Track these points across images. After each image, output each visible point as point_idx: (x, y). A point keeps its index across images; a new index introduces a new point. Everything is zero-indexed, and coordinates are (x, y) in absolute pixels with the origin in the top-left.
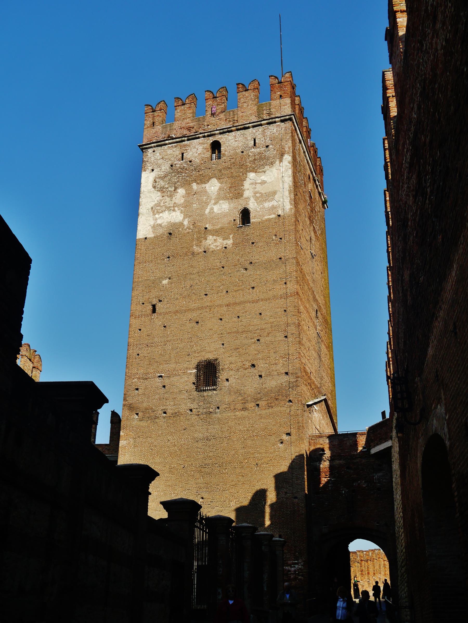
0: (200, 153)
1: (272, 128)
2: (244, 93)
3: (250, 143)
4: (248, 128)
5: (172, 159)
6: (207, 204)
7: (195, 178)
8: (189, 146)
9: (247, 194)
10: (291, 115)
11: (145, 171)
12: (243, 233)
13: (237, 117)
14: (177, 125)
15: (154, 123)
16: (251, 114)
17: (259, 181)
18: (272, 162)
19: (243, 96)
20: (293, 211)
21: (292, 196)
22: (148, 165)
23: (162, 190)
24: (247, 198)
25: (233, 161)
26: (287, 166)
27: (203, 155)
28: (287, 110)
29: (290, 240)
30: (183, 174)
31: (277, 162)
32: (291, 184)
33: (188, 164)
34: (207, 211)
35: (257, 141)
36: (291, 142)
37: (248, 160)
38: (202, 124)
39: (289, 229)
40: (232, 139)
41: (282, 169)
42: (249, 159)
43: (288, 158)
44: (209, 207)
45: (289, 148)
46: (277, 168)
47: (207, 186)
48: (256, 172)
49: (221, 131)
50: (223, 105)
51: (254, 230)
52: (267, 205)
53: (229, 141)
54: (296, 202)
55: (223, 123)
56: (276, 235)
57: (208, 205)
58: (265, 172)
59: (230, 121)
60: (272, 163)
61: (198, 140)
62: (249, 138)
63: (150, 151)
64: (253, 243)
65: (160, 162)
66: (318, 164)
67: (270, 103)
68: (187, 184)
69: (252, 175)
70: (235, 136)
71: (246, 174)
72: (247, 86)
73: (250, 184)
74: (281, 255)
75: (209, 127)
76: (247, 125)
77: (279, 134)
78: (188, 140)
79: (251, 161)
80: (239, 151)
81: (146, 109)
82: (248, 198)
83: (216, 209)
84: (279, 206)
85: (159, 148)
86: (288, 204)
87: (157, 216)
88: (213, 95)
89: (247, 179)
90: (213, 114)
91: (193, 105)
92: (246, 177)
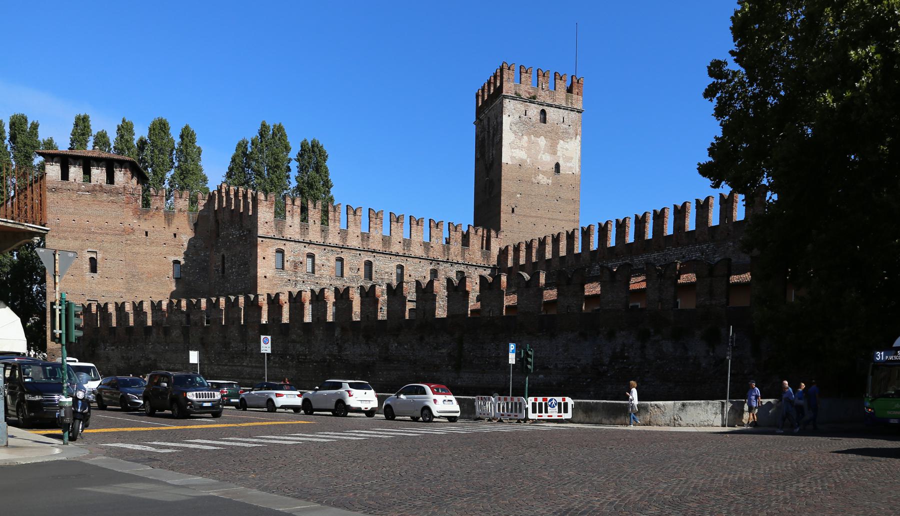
9: (559, 153)
23: (515, 132)
31: (574, 139)
34: (539, 157)
43: (579, 137)
44: (540, 155)
47: (539, 140)
60: (571, 138)
68: (529, 134)
69: (561, 142)
80: (556, 122)
87: (512, 150)
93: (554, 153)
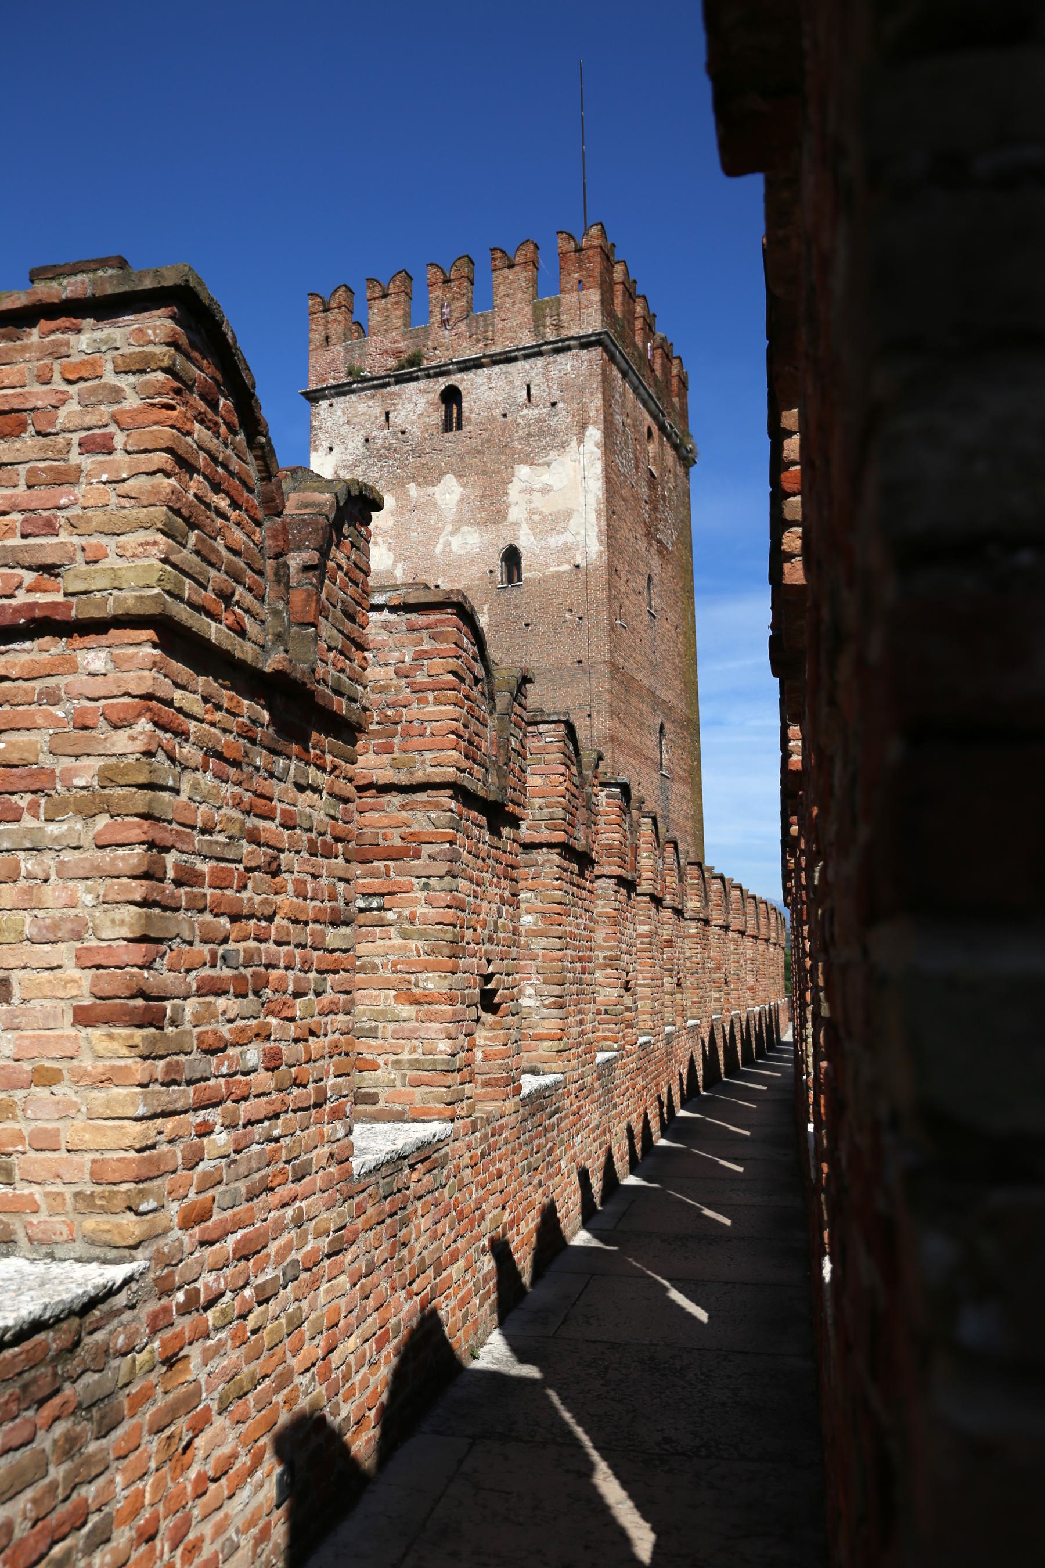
0: (422, 414)
1: (563, 361)
2: (505, 271)
3: (519, 395)
4: (515, 359)
5: (368, 425)
6: (438, 532)
7: (413, 471)
8: (399, 395)
9: (514, 514)
10: (600, 334)
11: (316, 450)
12: (508, 600)
13: (493, 332)
14: (375, 343)
15: (327, 338)
16: (521, 326)
17: (538, 486)
18: (563, 443)
19: (505, 278)
20: (605, 558)
21: (604, 523)
22: (322, 436)
24: (515, 524)
25: (486, 435)
26: (592, 453)
27: (427, 420)
28: (592, 322)
29: (598, 623)
30: (391, 462)
31: (574, 443)
32: (600, 494)
33: (398, 439)
34: (439, 548)
35: (533, 392)
36: (600, 396)
37: (516, 436)
38: (424, 346)
39: (596, 598)
40: (483, 384)
41: (584, 461)
42: (517, 432)
43: (594, 434)
44: (442, 540)
45: (597, 411)
46: (574, 458)
47: (437, 490)
48: (532, 464)
49: (461, 366)
50: (465, 299)
51: (529, 597)
52: (555, 541)
53: (478, 388)
54: (611, 537)
55: (464, 345)
56: (571, 611)
57: (439, 534)
58: (549, 464)
59: (478, 341)
60: (563, 445)
61: (416, 383)
62: (517, 383)
63: (324, 404)
64: (527, 625)
65: (345, 430)
66: (675, 372)
67: (559, 300)
69: (523, 471)
70: (489, 378)
71: (512, 468)
72: (510, 254)
73: (520, 492)
74: (582, 654)
75: (437, 352)
76: (513, 354)
77: (577, 376)
78: (397, 383)
79: (521, 438)
80: (498, 412)
81: (310, 302)
82: (516, 523)
83: (456, 543)
84: (577, 545)
85: (342, 398)
86: (595, 541)
88: (444, 274)
89: (515, 479)
90: (444, 323)
91: (403, 297)
92: (513, 476)
93: (498, 515)
